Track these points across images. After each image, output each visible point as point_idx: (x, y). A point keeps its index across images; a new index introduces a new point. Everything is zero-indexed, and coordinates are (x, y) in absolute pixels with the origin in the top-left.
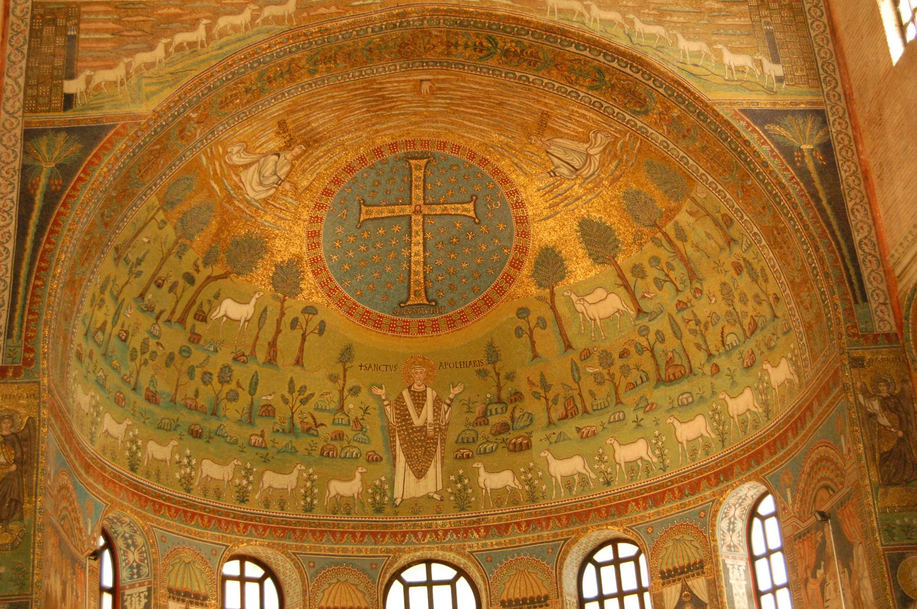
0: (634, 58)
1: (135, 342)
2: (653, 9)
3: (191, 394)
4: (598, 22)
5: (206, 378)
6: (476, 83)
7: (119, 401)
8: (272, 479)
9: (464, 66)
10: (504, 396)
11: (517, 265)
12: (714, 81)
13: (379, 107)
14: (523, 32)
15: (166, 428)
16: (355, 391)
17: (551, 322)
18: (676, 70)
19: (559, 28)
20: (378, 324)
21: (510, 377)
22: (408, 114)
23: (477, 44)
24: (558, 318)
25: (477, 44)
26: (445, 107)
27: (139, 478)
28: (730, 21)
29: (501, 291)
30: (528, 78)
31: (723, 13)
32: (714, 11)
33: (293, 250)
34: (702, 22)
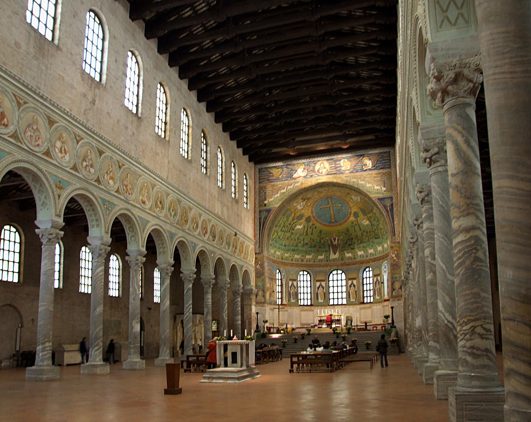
1: (281, 237)
3: (292, 243)
5: (295, 240)
7: (279, 248)
8: (308, 257)
10: (350, 238)
11: (350, 214)
15: (288, 251)
16: (323, 238)
17: (357, 225)
20: (326, 225)
21: (351, 235)
24: (359, 224)
27: (283, 261)
28: (377, 178)
29: (348, 219)
33: (308, 215)
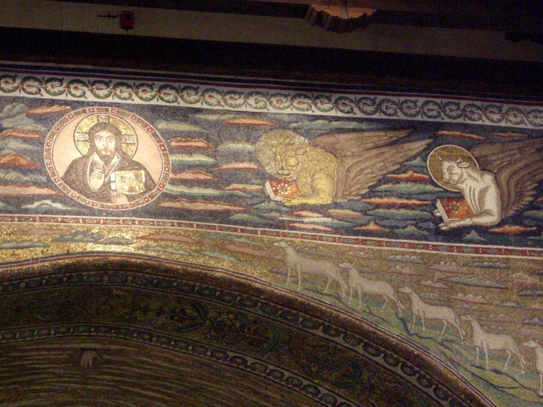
0: (409, 355)
2: (440, 280)
4: (360, 296)
6: (165, 359)
9: (152, 336)
12: (523, 397)
13: (12, 380)
14: (248, 303)
18: (469, 378)
19: (302, 303)
22: (53, 390)
23: (177, 310)
25: (177, 310)
26: (112, 386)
30: (245, 361)
31: (538, 292)
32: (526, 288)
34: (508, 304)
